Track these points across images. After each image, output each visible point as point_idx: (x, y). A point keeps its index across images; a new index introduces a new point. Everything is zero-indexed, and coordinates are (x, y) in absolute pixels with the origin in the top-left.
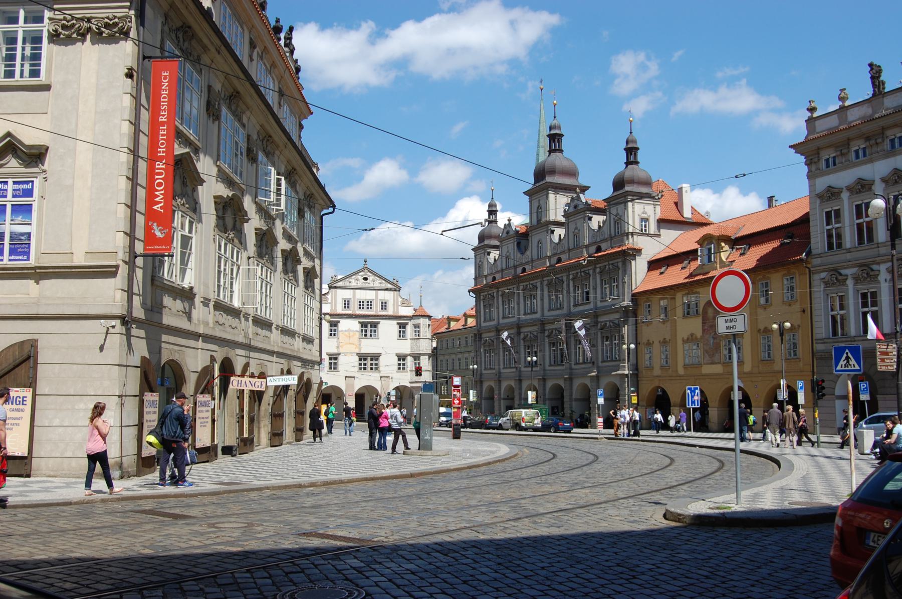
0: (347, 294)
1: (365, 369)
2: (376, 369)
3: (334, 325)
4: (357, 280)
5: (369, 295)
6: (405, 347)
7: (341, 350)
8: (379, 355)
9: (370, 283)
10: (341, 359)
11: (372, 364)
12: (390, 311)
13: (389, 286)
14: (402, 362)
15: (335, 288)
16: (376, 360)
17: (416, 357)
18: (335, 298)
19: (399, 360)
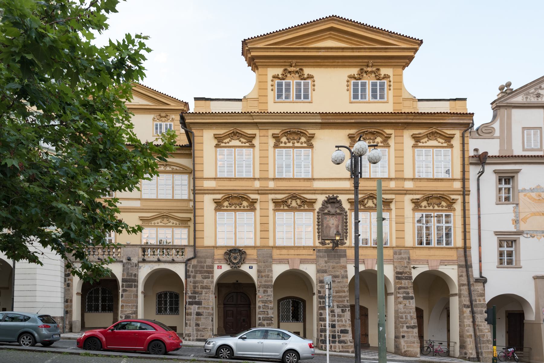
3: (507, 179)
7: (523, 227)
10: (525, 245)
18: (507, 128)
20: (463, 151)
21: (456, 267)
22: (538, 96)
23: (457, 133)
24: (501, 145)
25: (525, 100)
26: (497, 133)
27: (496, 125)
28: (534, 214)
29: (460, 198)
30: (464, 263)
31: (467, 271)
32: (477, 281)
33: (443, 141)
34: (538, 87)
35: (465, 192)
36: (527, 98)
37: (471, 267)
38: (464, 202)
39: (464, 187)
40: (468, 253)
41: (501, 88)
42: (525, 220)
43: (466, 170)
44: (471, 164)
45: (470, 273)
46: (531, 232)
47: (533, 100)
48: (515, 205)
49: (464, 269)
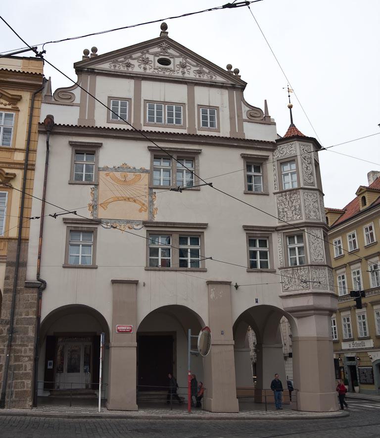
0: (124, 88)
1: (166, 264)
2: (195, 264)
4: (146, 62)
5: (177, 94)
6: (266, 212)
7: (102, 214)
8: (204, 226)
9: (175, 68)
11: (183, 253)
12: (225, 131)
13: (219, 79)
14: (258, 248)
15: (92, 72)
16: (195, 240)
17: (294, 233)
19: (251, 242)
20: (31, 116)
21: (5, 265)
22: (128, 65)
23: (26, 96)
24: (82, 113)
25: (113, 68)
26: (77, 100)
27: (77, 92)
28: (118, 199)
29: (20, 173)
30: (14, 260)
31: (17, 271)
32: (29, 286)
33: (7, 103)
34: (128, 56)
35: (28, 167)
36: (115, 66)
37: (25, 264)
38: (25, 179)
39: (27, 159)
40: (23, 246)
41: (86, 52)
42: (105, 205)
43: (32, 138)
44: (40, 132)
45: (20, 275)
46: (113, 221)
47: (122, 68)
48: (93, 186)
49: (13, 269)
